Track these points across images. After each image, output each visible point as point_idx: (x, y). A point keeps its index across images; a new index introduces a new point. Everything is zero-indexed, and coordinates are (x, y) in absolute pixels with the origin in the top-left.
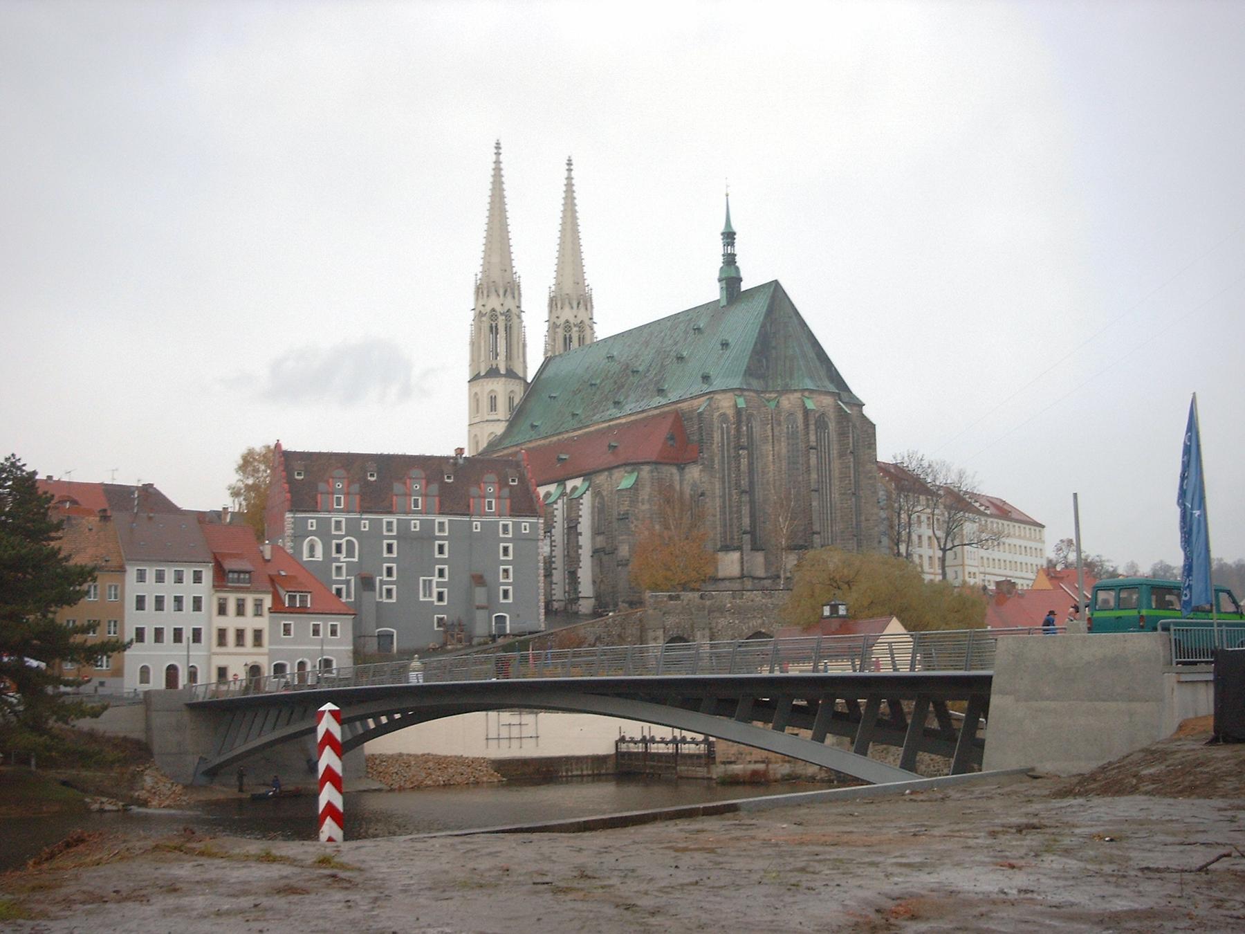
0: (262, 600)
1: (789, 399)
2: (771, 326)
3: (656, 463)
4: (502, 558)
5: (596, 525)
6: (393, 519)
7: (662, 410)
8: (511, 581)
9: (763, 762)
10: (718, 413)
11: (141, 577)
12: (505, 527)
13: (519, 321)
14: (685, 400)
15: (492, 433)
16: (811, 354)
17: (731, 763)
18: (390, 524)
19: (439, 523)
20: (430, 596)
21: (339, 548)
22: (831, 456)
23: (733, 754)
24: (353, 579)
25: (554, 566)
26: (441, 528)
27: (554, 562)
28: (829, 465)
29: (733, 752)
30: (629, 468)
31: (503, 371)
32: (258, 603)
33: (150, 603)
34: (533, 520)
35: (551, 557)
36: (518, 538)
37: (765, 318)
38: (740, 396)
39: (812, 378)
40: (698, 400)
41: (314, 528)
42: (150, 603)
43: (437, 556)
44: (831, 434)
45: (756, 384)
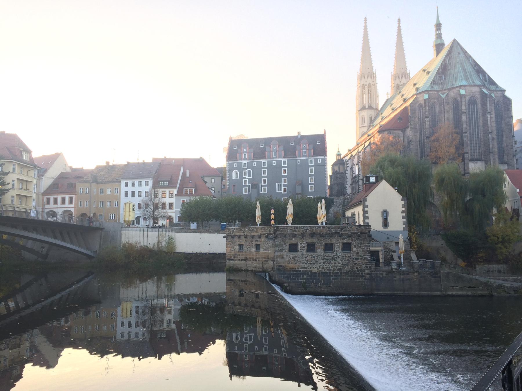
1: (453, 92)
2: (449, 60)
6: (265, 161)
9: (245, 260)
10: (418, 104)
11: (127, 184)
13: (373, 87)
15: (363, 132)
16: (469, 68)
17: (232, 260)
19: (284, 161)
20: (281, 190)
21: (245, 172)
22: (478, 116)
23: (233, 255)
24: (250, 185)
25: (359, 178)
27: (360, 177)
28: (477, 120)
29: (233, 254)
31: (367, 107)
33: (130, 194)
34: (323, 157)
35: (358, 174)
36: (316, 165)
37: (446, 57)
38: (427, 94)
39: (467, 79)
41: (236, 167)
42: (130, 194)
44: (478, 105)
45: (436, 87)
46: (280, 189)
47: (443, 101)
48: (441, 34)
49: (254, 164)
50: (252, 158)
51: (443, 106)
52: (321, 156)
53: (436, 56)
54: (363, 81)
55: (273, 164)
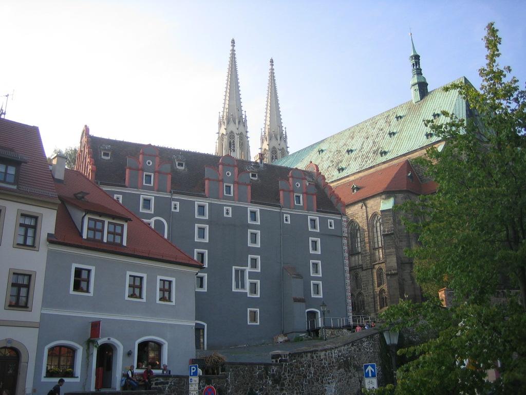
0: (36, 218)
3: (407, 191)
4: (311, 252)
5: (350, 248)
6: (206, 203)
12: (313, 221)
14: (415, 151)
18: (201, 207)
20: (243, 287)
26: (254, 218)
30: (383, 196)
32: (27, 221)
34: (338, 217)
36: (325, 235)
43: (250, 245)
46: (241, 283)
48: (421, 70)
49: (173, 206)
50: (169, 188)
52: (330, 213)
53: (421, 100)
54: (233, 128)
55: (225, 215)
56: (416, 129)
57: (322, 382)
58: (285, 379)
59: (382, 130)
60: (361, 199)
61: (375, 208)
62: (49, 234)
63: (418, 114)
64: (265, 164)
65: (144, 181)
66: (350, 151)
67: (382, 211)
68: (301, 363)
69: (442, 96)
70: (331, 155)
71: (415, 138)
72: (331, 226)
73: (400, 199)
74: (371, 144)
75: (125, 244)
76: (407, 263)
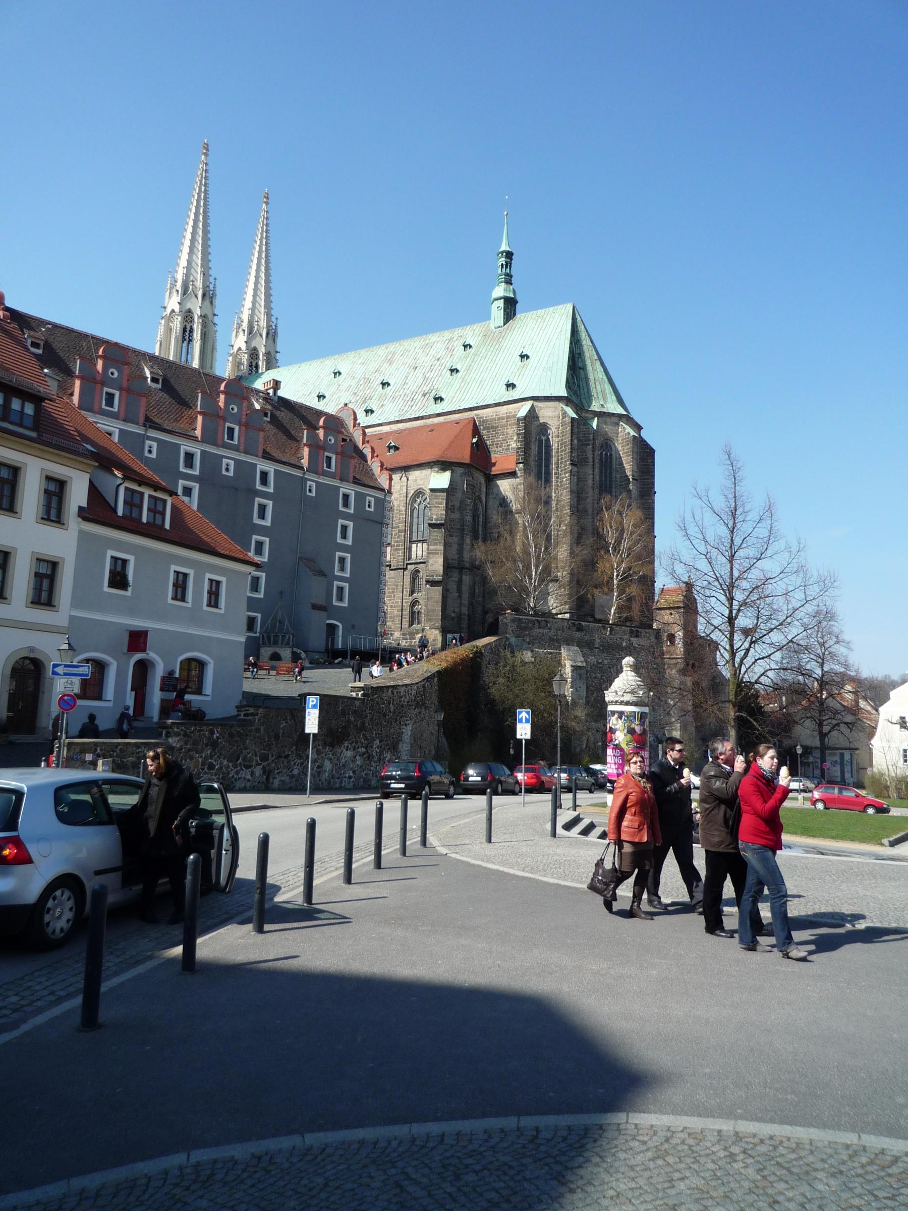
4: (339, 540)
7: (449, 417)
8: (348, 575)
12: (346, 497)
36: (360, 517)
40: (505, 407)
47: (592, 436)
48: (511, 276)
49: (147, 449)
50: (142, 419)
51: (590, 447)
53: (505, 324)
55: (224, 472)
56: (491, 372)
57: (400, 723)
58: (366, 717)
59: (438, 359)
60: (401, 465)
61: (422, 482)
62: (80, 507)
63: (497, 346)
64: (280, 398)
65: (104, 402)
66: (385, 384)
67: (432, 490)
68: (382, 699)
69: (536, 327)
70: (354, 383)
71: (489, 384)
72: (369, 506)
73: (459, 475)
74: (420, 380)
75: (167, 526)
76: (455, 568)
